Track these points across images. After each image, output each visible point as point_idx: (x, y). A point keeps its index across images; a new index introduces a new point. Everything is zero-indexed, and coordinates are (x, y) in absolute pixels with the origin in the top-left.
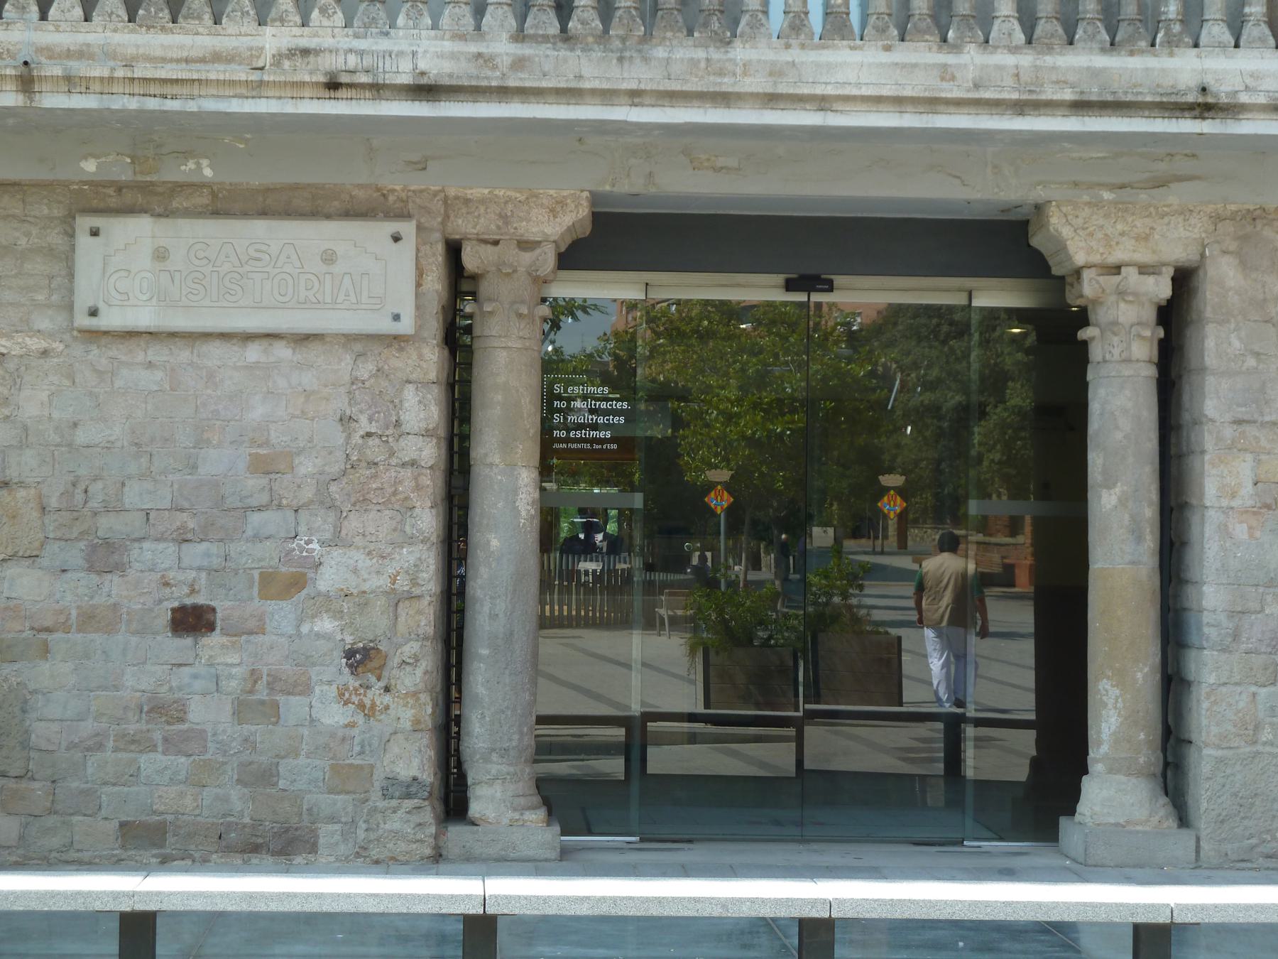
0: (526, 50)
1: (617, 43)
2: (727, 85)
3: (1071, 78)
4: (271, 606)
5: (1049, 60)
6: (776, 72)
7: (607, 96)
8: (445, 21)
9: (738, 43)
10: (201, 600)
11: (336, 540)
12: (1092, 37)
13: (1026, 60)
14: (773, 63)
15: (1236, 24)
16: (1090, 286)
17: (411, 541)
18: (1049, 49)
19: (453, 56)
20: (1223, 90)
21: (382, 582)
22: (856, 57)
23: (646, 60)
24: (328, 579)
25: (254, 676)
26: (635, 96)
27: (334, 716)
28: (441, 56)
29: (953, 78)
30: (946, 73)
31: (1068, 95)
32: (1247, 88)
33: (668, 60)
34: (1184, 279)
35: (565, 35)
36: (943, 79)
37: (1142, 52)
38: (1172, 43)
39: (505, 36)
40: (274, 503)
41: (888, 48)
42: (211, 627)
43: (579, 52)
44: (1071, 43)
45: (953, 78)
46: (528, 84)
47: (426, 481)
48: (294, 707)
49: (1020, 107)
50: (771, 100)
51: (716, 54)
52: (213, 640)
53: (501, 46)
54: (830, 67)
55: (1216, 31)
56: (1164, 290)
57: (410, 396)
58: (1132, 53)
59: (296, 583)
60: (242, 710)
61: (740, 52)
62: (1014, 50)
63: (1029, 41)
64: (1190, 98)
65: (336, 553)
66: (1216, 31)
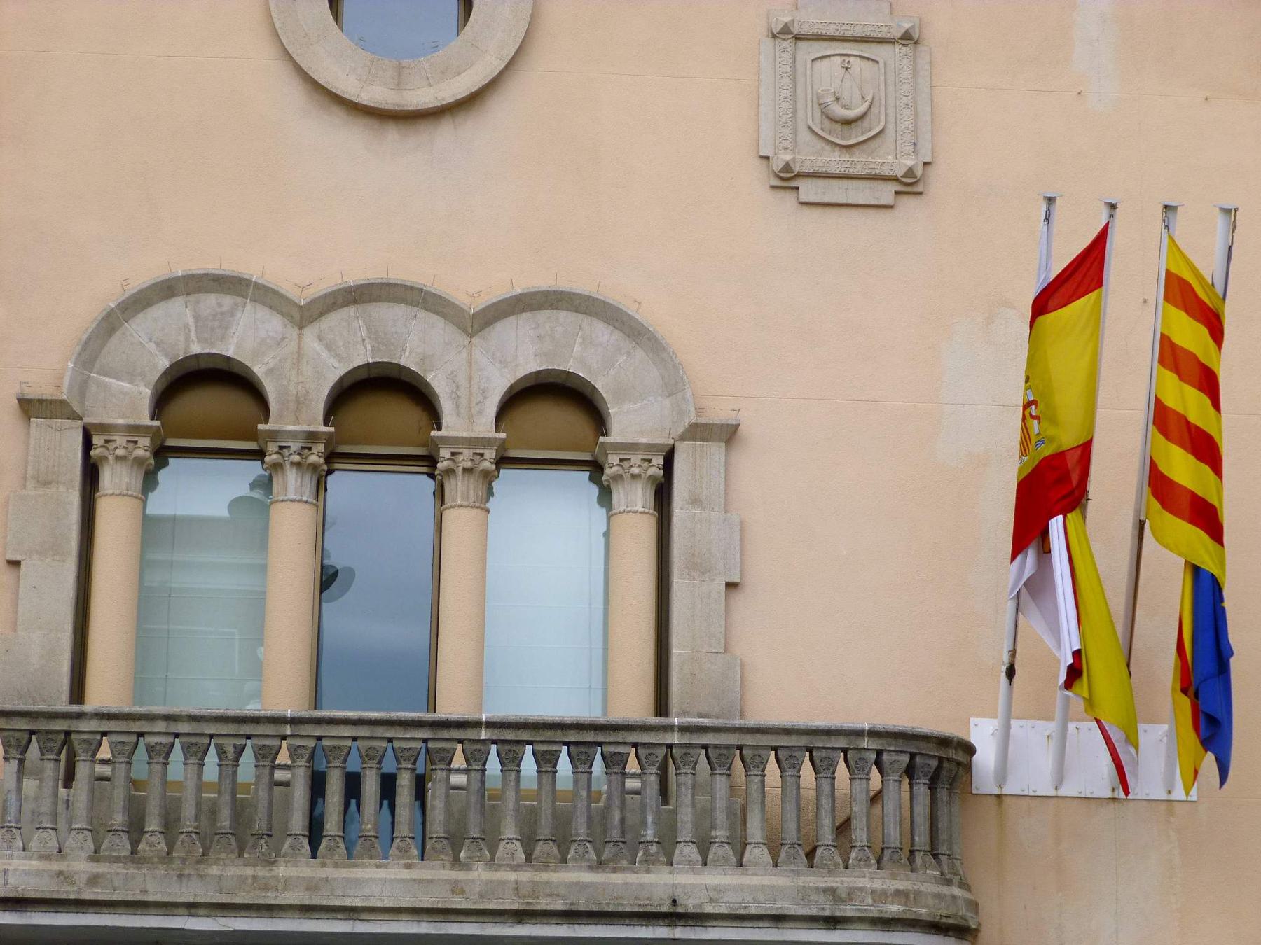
0: (101, 868)
1: (178, 863)
2: (270, 898)
3: (562, 892)
5: (544, 876)
6: (312, 886)
7: (167, 907)
8: (34, 845)
9: (281, 860)
12: (582, 857)
13: (525, 876)
14: (311, 879)
15: (704, 845)
18: (546, 867)
19: (38, 873)
20: (690, 904)
22: (382, 873)
23: (202, 877)
26: (192, 908)
28: (27, 873)
29: (463, 892)
30: (457, 888)
31: (559, 906)
32: (711, 900)
33: (220, 877)
35: (135, 857)
36: (453, 892)
37: (623, 870)
38: (649, 862)
39: (84, 855)
41: (408, 866)
43: (144, 871)
44: (564, 860)
45: (463, 892)
46: (100, 897)
49: (521, 916)
50: (307, 910)
51: (261, 872)
53: (81, 866)
54: (356, 881)
55: (687, 851)
58: (615, 870)
61: (282, 871)
62: (516, 868)
63: (529, 858)
64: (665, 909)
66: (687, 851)
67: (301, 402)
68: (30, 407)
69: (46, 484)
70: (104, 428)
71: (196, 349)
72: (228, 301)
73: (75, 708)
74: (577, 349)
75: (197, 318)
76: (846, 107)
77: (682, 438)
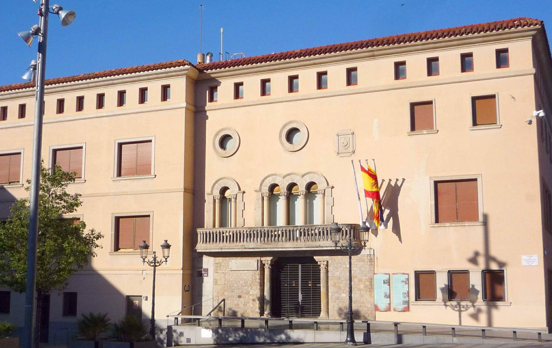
4: (246, 295)
10: (240, 295)
11: (251, 289)
16: (319, 263)
17: (257, 289)
21: (255, 293)
24: (251, 293)
25: (245, 302)
27: (251, 306)
34: (328, 262)
40: (246, 286)
42: (241, 297)
47: (259, 283)
48: (248, 305)
52: (241, 298)
56: (325, 263)
57: (257, 276)
59: (248, 293)
60: (244, 305)
65: (251, 290)
67: (284, 188)
68: (256, 191)
69: (258, 200)
70: (263, 193)
71: (273, 183)
72: (276, 176)
73: (263, 227)
74: (314, 179)
75: (272, 179)
76: (345, 144)
77: (326, 188)
